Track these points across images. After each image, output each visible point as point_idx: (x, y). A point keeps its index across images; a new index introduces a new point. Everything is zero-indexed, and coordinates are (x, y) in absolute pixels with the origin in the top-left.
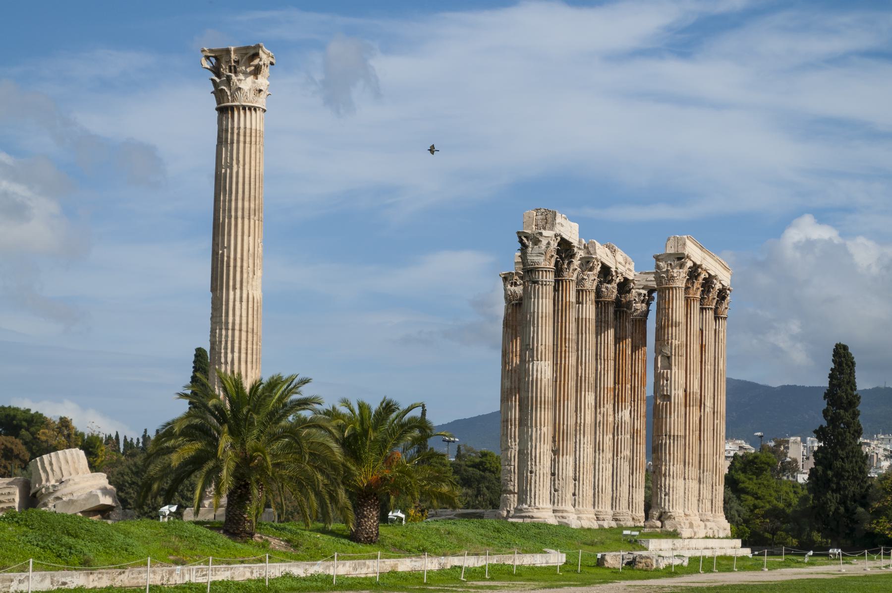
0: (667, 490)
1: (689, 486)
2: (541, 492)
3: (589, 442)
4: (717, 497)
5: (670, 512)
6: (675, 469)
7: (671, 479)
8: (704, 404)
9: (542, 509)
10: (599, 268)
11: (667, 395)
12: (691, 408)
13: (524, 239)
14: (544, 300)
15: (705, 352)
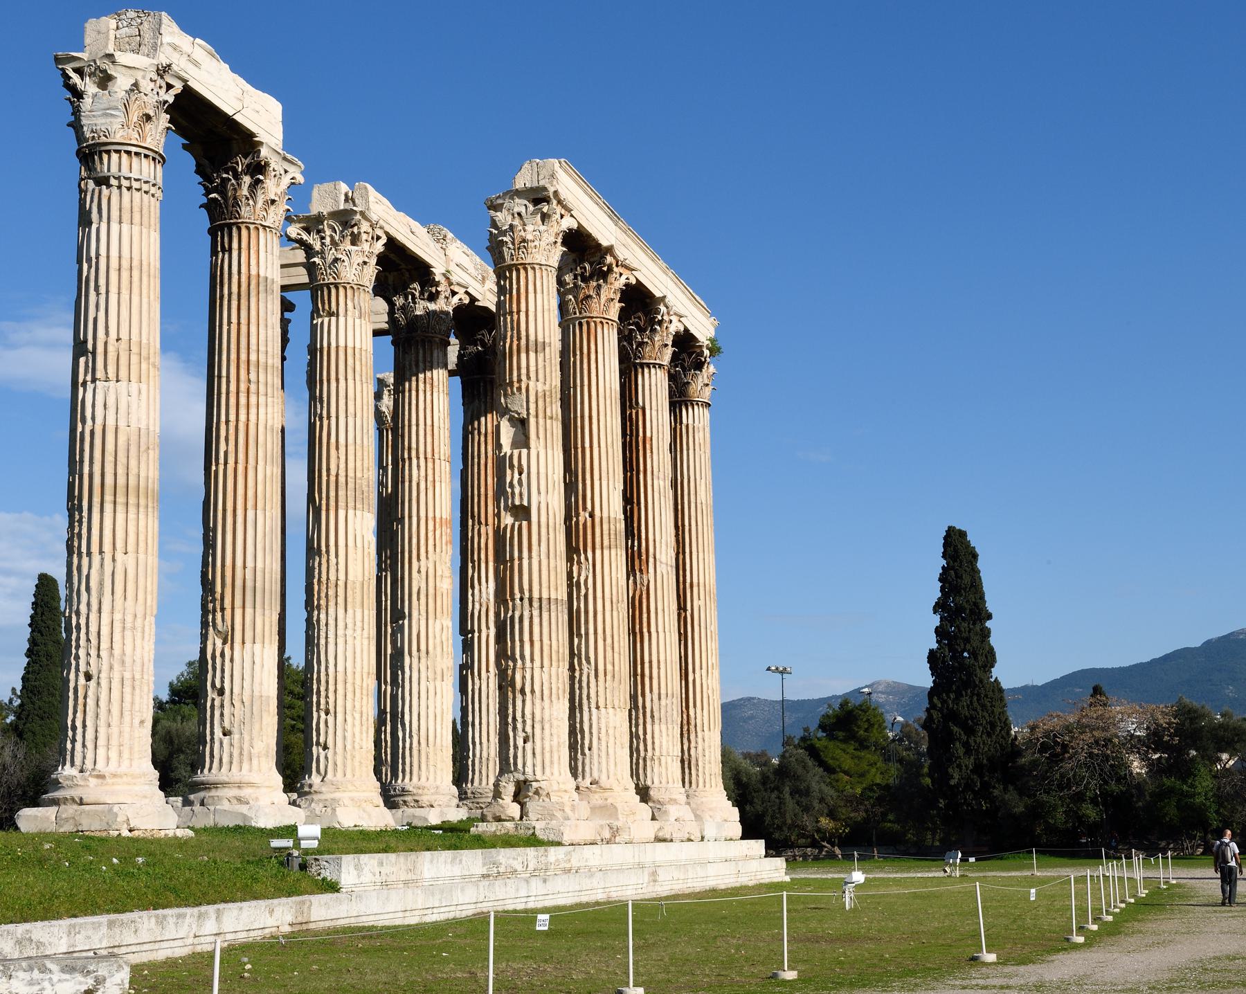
0: (528, 729)
1: (607, 723)
2: (114, 730)
3: (359, 624)
4: (707, 753)
5: (537, 781)
6: (546, 677)
7: (538, 701)
8: (655, 558)
9: (115, 776)
10: (379, 247)
11: (522, 506)
12: (606, 552)
13: (72, 74)
14: (125, 227)
15: (652, 452)
